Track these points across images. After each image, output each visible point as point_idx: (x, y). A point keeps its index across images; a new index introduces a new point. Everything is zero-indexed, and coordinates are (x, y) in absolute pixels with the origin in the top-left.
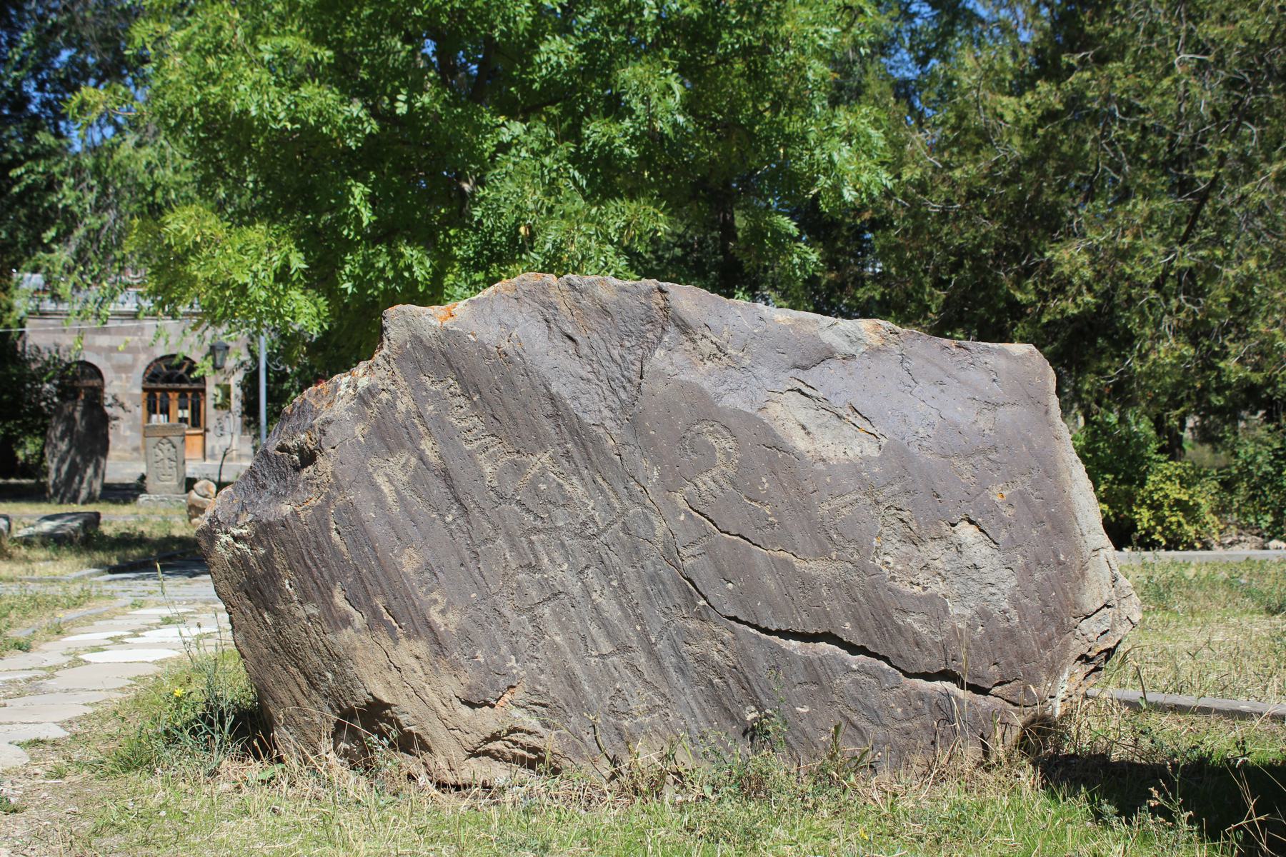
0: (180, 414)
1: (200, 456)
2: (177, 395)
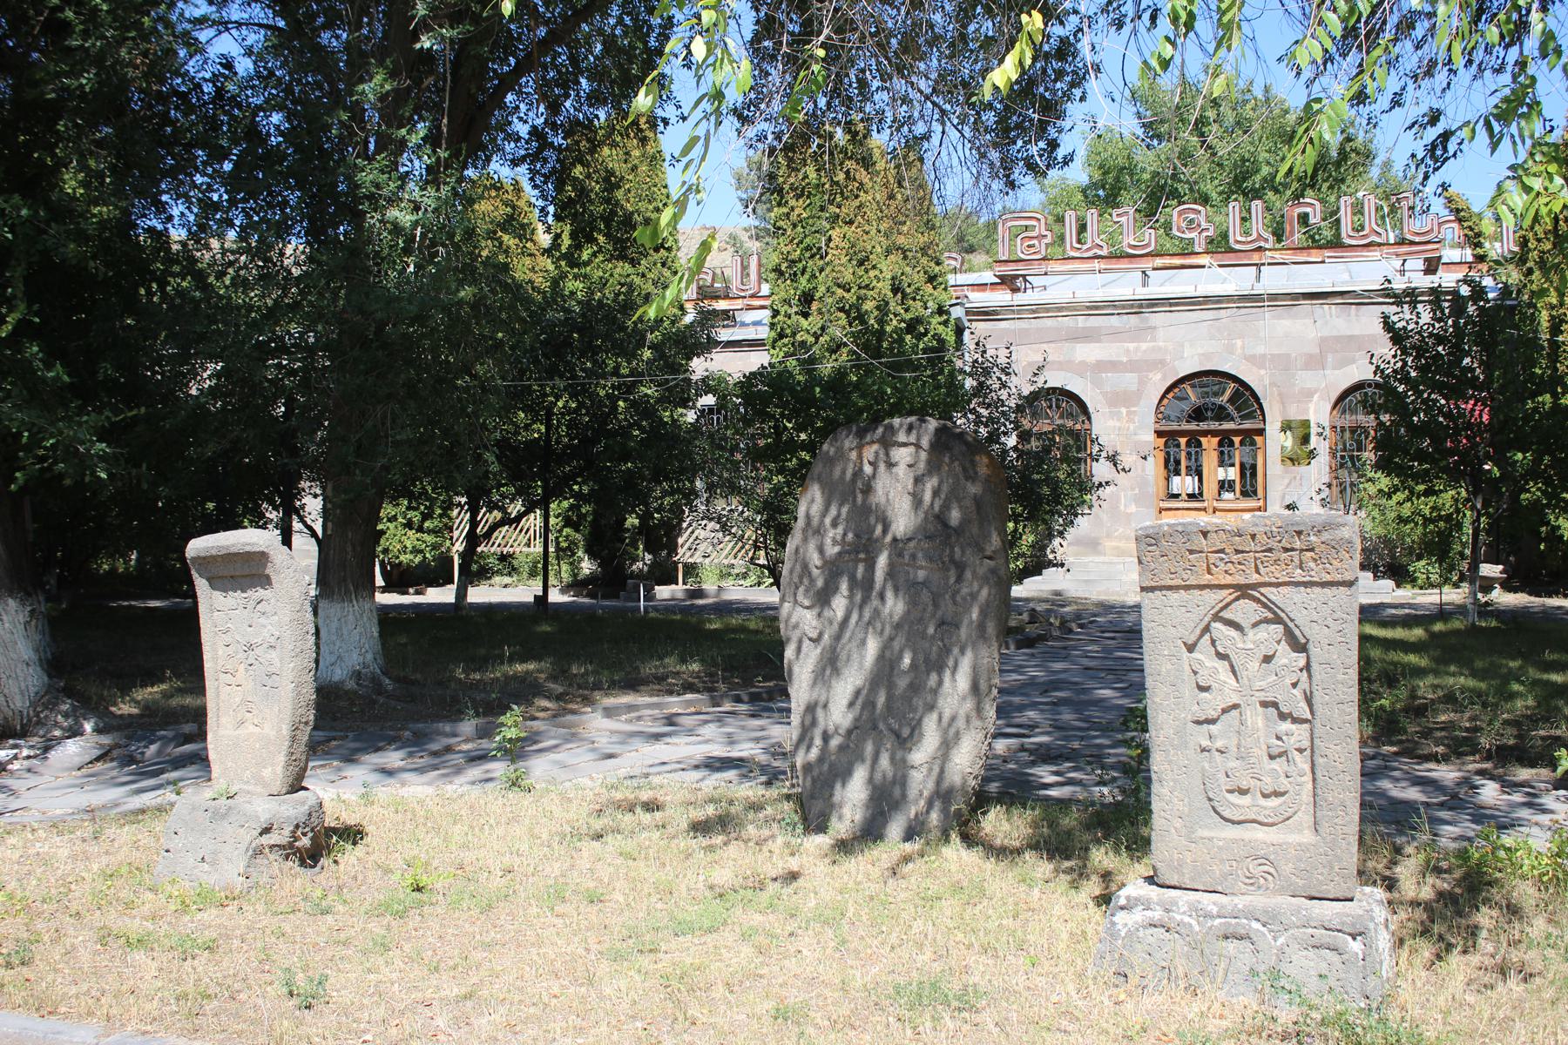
0: (1221, 474)
2: (1215, 440)
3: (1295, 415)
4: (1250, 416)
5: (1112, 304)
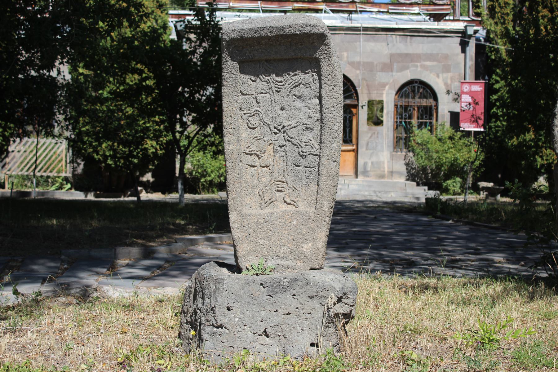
1: (352, 172)
3: (375, 97)
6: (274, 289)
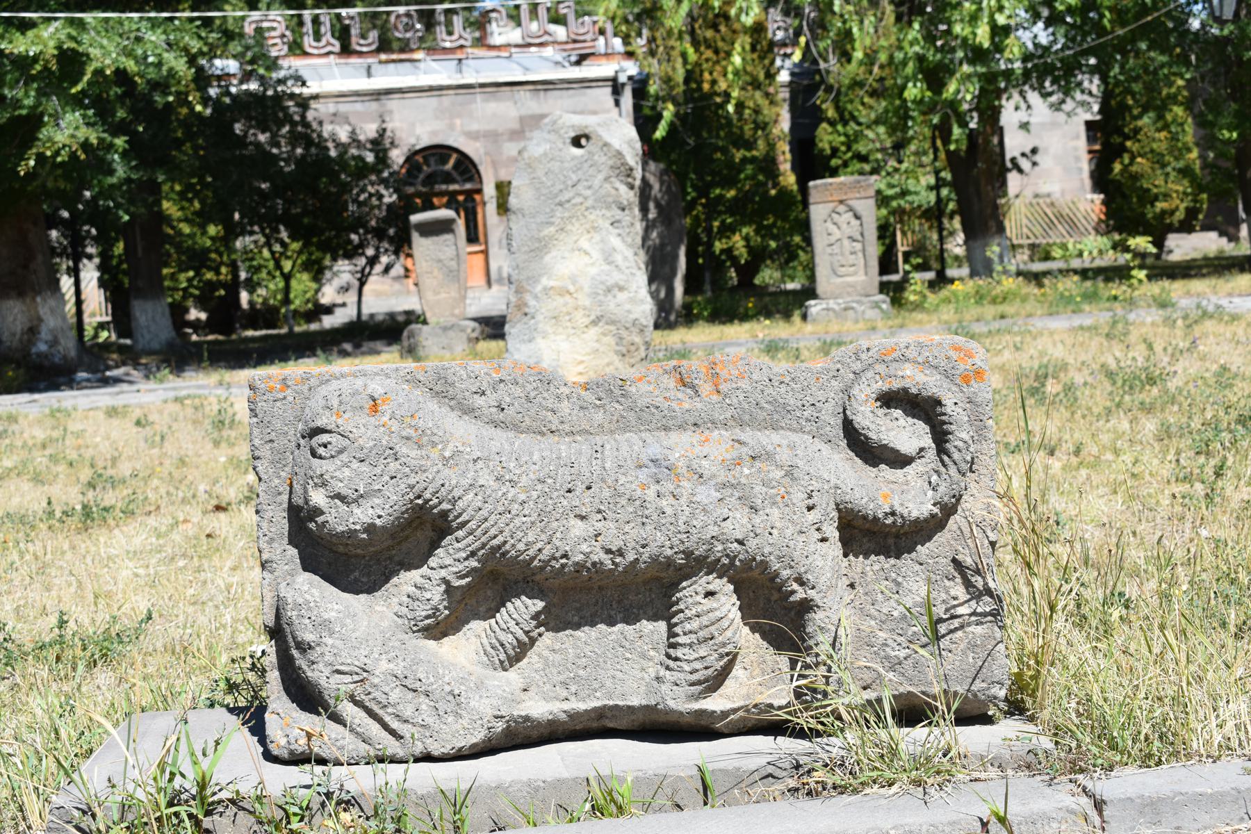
1: (482, 281)
3: (504, 176)
4: (470, 179)
5: (357, 94)
6: (445, 329)
